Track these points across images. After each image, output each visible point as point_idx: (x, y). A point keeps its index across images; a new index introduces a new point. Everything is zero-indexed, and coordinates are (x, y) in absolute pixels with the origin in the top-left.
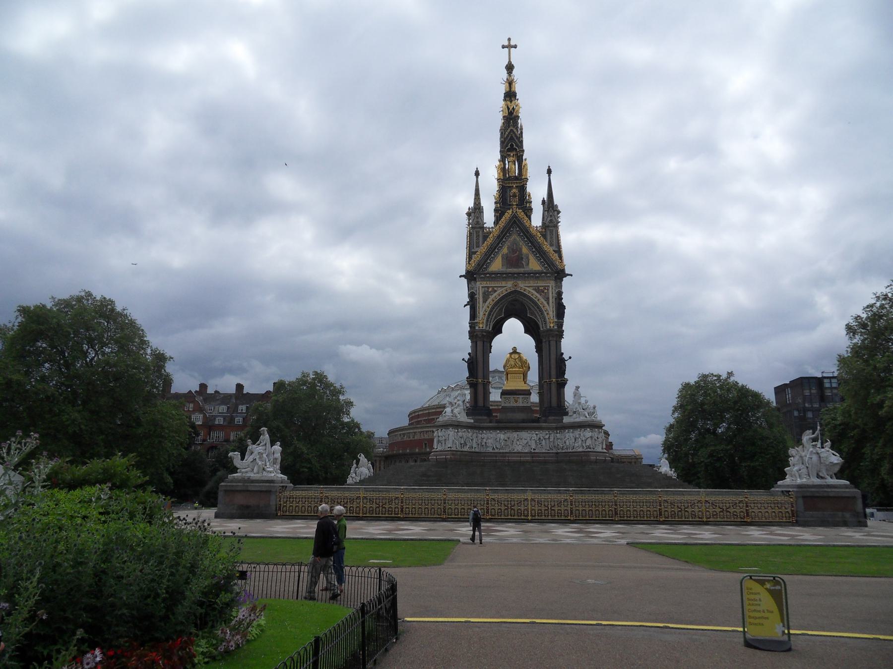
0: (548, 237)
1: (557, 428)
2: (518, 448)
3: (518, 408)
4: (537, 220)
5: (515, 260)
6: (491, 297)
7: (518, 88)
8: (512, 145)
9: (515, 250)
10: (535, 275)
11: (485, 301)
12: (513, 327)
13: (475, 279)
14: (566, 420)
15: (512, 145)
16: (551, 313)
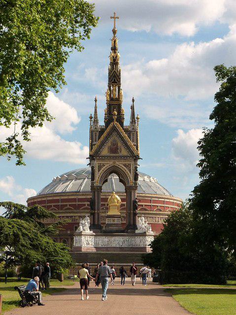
0: (132, 137)
1: (132, 236)
2: (114, 245)
3: (114, 224)
4: (127, 122)
5: (114, 150)
6: (103, 169)
7: (118, 46)
8: (115, 80)
9: (114, 144)
10: (124, 158)
11: (99, 171)
12: (115, 178)
13: (94, 159)
14: (137, 232)
15: (115, 80)
16: (131, 178)
